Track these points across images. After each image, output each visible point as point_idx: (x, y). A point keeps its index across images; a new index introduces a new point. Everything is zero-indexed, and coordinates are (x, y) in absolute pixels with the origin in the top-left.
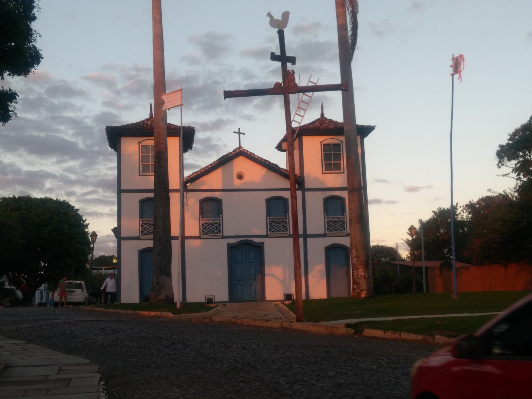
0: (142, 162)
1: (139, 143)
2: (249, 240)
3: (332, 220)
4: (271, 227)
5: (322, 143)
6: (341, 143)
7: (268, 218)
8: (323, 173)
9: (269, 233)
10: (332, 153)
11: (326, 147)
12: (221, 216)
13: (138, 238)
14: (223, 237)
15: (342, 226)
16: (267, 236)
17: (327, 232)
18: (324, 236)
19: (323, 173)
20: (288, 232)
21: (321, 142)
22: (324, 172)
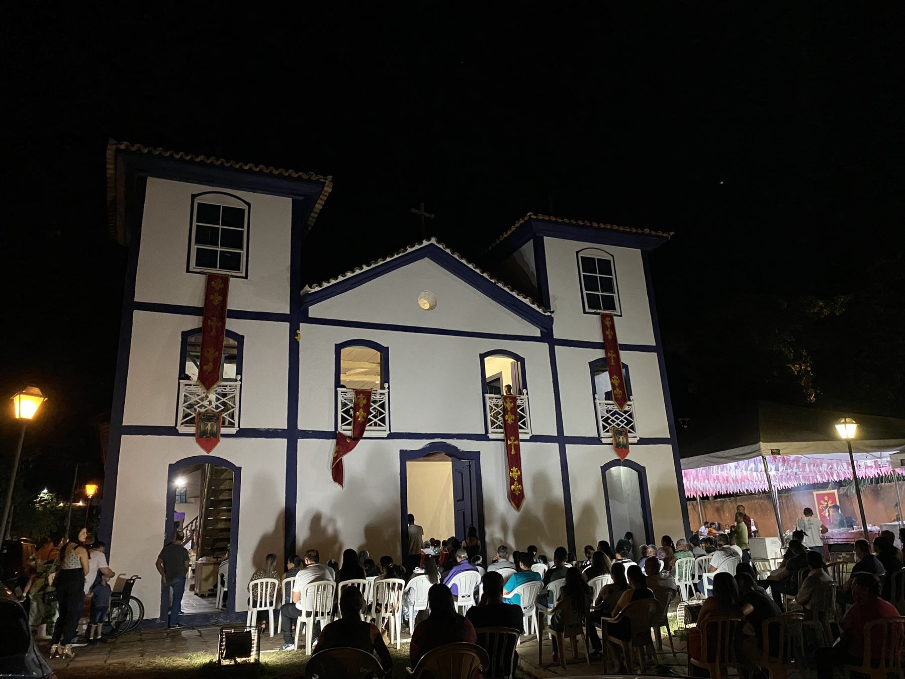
0: (197, 242)
1: (194, 197)
2: (449, 445)
3: (610, 408)
4: (494, 416)
5: (580, 255)
6: (611, 259)
7: (487, 395)
8: (585, 312)
9: (490, 429)
10: (598, 275)
11: (587, 264)
12: (386, 385)
13: (171, 431)
14: (392, 436)
15: (629, 422)
16: (484, 437)
17: (603, 434)
18: (597, 441)
19: (585, 312)
20: (529, 431)
21: (577, 253)
22: (587, 310)
